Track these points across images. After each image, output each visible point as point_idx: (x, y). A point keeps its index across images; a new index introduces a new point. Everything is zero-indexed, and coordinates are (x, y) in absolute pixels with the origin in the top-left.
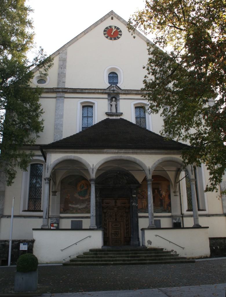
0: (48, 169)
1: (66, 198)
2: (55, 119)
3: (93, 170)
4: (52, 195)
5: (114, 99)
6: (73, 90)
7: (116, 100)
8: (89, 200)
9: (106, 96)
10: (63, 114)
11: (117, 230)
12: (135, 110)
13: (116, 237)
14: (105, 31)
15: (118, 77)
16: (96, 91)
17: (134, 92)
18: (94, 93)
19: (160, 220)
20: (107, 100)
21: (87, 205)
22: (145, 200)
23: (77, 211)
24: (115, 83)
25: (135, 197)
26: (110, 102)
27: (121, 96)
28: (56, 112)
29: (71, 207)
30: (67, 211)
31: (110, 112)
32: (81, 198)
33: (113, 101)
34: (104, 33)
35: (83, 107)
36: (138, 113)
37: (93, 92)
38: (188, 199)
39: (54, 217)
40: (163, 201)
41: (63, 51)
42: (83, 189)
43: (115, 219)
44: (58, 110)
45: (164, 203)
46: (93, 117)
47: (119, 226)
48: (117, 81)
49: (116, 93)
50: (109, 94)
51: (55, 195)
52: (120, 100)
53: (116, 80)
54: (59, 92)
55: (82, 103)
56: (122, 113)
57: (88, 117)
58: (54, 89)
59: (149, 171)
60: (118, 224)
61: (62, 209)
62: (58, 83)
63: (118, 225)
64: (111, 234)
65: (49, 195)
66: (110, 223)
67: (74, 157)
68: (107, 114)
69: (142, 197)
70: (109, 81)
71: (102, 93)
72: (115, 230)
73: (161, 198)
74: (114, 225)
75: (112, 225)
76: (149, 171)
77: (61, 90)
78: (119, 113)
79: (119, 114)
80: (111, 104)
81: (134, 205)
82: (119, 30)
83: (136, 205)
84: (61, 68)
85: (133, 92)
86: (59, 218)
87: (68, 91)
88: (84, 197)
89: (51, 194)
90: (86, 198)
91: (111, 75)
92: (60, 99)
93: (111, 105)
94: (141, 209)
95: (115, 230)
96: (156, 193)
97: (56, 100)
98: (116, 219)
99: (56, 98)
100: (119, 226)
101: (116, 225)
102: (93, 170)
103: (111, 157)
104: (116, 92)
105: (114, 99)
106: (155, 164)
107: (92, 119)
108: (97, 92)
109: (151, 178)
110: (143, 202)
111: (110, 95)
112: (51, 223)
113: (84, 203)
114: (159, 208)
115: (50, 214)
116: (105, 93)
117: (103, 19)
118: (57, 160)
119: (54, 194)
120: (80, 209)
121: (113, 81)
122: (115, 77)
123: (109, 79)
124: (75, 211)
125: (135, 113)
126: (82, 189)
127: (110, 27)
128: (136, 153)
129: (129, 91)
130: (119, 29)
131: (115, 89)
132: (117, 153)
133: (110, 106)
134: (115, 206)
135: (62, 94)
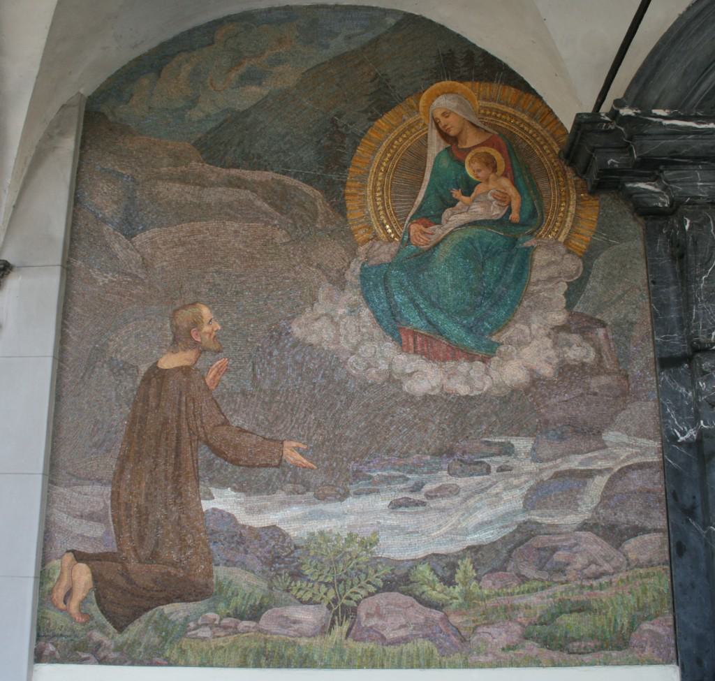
1: (157, 375)
21: (536, 497)
23: (344, 612)
29: (240, 538)
30: (176, 611)
42: (453, 219)
61: (83, 576)
88: (487, 353)
90: (512, 372)
113: (474, 466)
124: (307, 616)
126: (430, 215)
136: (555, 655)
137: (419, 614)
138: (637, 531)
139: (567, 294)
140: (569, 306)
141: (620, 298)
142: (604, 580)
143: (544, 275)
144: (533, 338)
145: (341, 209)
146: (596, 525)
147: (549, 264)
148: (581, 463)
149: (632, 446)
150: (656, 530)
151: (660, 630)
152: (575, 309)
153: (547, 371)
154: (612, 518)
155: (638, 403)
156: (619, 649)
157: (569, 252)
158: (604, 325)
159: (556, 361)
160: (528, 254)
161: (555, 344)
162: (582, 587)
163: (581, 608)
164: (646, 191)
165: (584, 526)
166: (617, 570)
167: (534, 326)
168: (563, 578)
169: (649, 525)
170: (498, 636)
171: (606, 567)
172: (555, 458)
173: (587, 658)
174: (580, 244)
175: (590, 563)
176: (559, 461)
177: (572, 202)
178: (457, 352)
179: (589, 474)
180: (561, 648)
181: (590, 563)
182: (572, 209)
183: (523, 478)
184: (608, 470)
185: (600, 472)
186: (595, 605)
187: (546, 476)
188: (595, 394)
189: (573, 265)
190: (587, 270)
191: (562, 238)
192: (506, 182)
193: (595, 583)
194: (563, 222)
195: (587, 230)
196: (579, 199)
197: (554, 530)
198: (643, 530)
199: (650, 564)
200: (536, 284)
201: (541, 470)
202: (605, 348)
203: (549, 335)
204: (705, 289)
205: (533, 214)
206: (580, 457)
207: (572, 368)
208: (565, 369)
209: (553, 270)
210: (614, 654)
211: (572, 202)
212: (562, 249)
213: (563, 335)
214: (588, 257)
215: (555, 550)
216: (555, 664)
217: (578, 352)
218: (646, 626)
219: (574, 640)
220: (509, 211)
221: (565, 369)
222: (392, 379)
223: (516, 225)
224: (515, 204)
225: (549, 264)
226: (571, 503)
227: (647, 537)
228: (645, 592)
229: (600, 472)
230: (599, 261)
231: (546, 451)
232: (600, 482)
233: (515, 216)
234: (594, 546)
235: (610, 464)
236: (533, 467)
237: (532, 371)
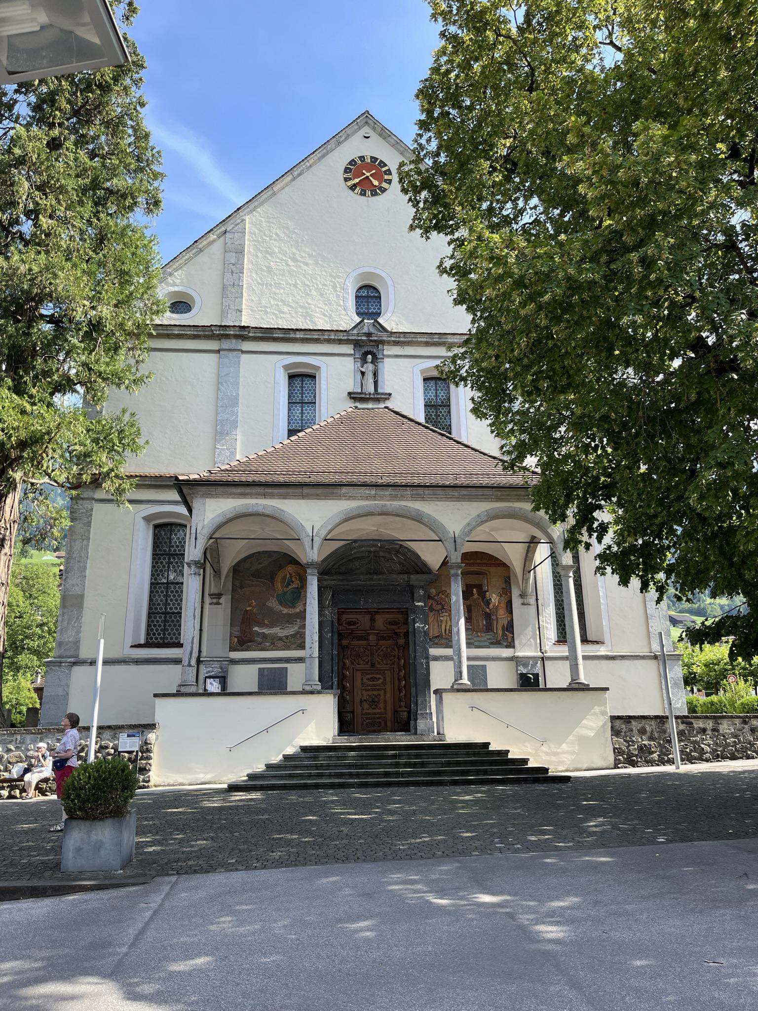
0: (196, 539)
1: (246, 611)
2: (217, 406)
3: (312, 540)
4: (210, 604)
5: (370, 357)
6: (262, 333)
7: (375, 360)
8: (302, 615)
9: (349, 349)
10: (238, 395)
11: (376, 693)
12: (424, 387)
13: (373, 709)
14: (347, 170)
15: (380, 297)
16: (324, 335)
17: (423, 340)
18: (317, 341)
19: (484, 667)
20: (351, 359)
22: (447, 614)
24: (372, 313)
26: (359, 364)
27: (389, 350)
28: (218, 389)
29: (259, 634)
30: (249, 644)
31: (360, 391)
32: (285, 611)
33: (366, 363)
34: (346, 176)
35: (291, 377)
36: (432, 394)
37: (317, 337)
38: (556, 614)
39: (215, 659)
40: (494, 617)
41: (236, 225)
42: (290, 587)
44: (225, 384)
45: (495, 623)
46: (315, 403)
47: (381, 681)
48: (379, 309)
49: (375, 341)
50: (357, 344)
51: (218, 604)
52: (386, 360)
53: (376, 306)
54: (227, 336)
55: (286, 367)
56: (390, 394)
57: (302, 403)
58: (213, 328)
59: (455, 541)
60: (378, 676)
61: (236, 639)
62: (223, 313)
64: (361, 702)
65: (203, 602)
66: (358, 675)
67: (265, 506)
68: (354, 397)
69: (439, 607)
70: (357, 308)
71: (340, 342)
72: (370, 693)
73: (488, 610)
74: (368, 679)
75: (362, 679)
76: (455, 541)
77: (232, 333)
78: (382, 394)
79: (383, 396)
80: (363, 370)
81: (419, 627)
82: (384, 169)
83: (423, 628)
84: (232, 272)
85: (419, 340)
86: (226, 663)
87: (250, 335)
88: (294, 607)
89: (207, 600)
90: (298, 610)
91: (364, 292)
92: (231, 355)
93: (363, 373)
94: (438, 636)
95: (370, 693)
96: (476, 596)
97: (220, 358)
98: (373, 665)
99: (218, 351)
100: (381, 681)
101: (373, 679)
102: (312, 540)
103: (358, 507)
104: (376, 338)
105: (370, 357)
106: (468, 524)
107: (315, 410)
108: (326, 337)
109: (459, 560)
110: (442, 621)
111: (360, 346)
112: (206, 677)
114: (483, 635)
115: (204, 653)
116: (347, 342)
117: (344, 138)
118: (219, 515)
119: (215, 601)
120: (281, 639)
121: (368, 308)
122: (374, 297)
123: (357, 302)
124: (267, 644)
125: (424, 393)
127: (361, 160)
128: (423, 499)
129: (407, 335)
130: (385, 165)
131: (372, 330)
132: (374, 497)
133: (359, 375)
134: (371, 629)
135: (234, 341)
137: (283, 643)
145: (274, 586)
170: (294, 646)
178: (290, 607)
222: (281, 611)
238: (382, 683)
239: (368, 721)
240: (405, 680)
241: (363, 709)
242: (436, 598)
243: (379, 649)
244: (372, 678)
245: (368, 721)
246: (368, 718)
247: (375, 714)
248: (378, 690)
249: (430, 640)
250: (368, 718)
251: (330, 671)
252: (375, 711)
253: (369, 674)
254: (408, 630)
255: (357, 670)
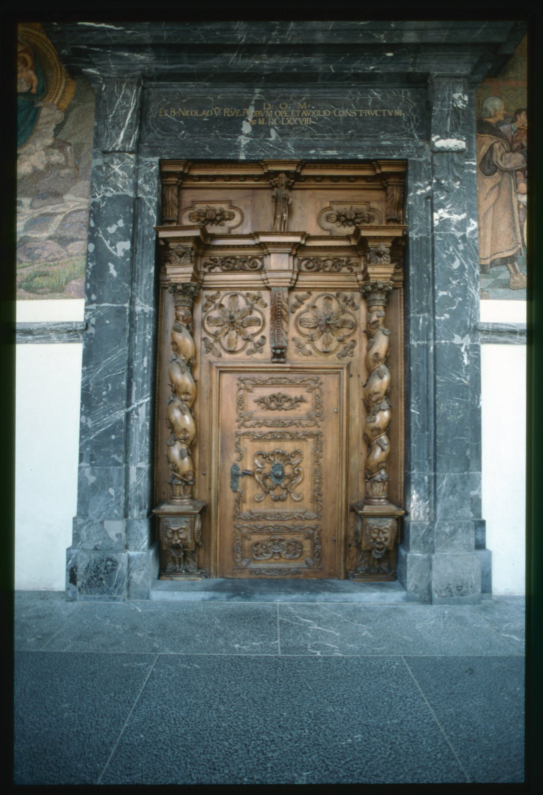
25: (460, 152)
43: (268, 348)
47: (305, 408)
60: (294, 393)
63: (301, 400)
64: (235, 476)
72: (270, 447)
75: (240, 402)
81: (445, 223)
83: (463, 225)
100: (305, 408)
136: (32, 295)
138: (73, 240)
139: (55, 130)
140: (55, 136)
141: (80, 131)
142: (56, 262)
143: (45, 120)
144: (36, 151)
146: (56, 238)
147: (48, 115)
148: (52, 209)
149: (76, 201)
150: (82, 240)
151: (79, 284)
152: (58, 137)
153: (41, 167)
154: (62, 235)
155: (82, 181)
156: (60, 292)
157: (58, 109)
158: (70, 144)
159: (46, 162)
160: (38, 110)
161: (47, 154)
162: (46, 265)
163: (45, 275)
164: (93, 74)
165: (50, 238)
166: (62, 258)
167: (38, 146)
168: (38, 261)
169: (80, 237)
171: (58, 256)
172: (41, 207)
173: (45, 296)
174: (64, 105)
175: (51, 254)
176: (42, 209)
177: (63, 83)
179: (54, 215)
180: (33, 292)
181: (51, 254)
182: (62, 87)
183: (26, 216)
184: (64, 212)
185: (60, 214)
186: (50, 273)
187: (36, 215)
188: (62, 178)
189: (59, 116)
190: (66, 118)
191: (56, 102)
192: (31, 73)
193: (52, 263)
194: (57, 94)
195: (69, 97)
196: (67, 82)
197: (36, 240)
198: (77, 240)
199: (78, 255)
200: (41, 125)
201: (34, 213)
202: (70, 156)
203: (44, 150)
204: (112, 122)
205: (43, 90)
206: (51, 207)
207: (53, 165)
208: (50, 166)
209: (49, 119)
210: (58, 294)
211: (63, 83)
212: (55, 108)
213: (50, 150)
214: (67, 112)
215: (36, 248)
216: (30, 299)
217: (57, 157)
218: (73, 282)
219: (40, 288)
220: (31, 88)
221: (50, 166)
223: (34, 95)
224: (35, 84)
225: (48, 115)
226: (46, 228)
227: (78, 242)
228: (74, 266)
229: (60, 214)
230: (73, 114)
231: (37, 204)
232: (60, 217)
233: (34, 91)
234: (54, 246)
235: (65, 210)
236: (30, 211)
237: (34, 167)
238: (309, 417)
239: (255, 538)
240: (391, 409)
241: (240, 500)
242: (504, 128)
243: (301, 301)
244: (274, 397)
245: (255, 538)
246: (260, 531)
247: (279, 517)
248: (294, 437)
249: (484, 269)
250: (260, 531)
251: (122, 371)
252: (279, 507)
253: (264, 384)
254: (405, 238)
255: (222, 371)
